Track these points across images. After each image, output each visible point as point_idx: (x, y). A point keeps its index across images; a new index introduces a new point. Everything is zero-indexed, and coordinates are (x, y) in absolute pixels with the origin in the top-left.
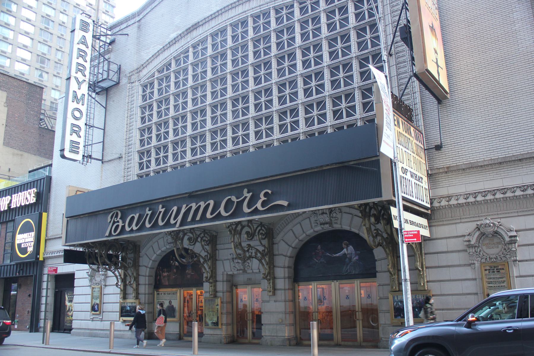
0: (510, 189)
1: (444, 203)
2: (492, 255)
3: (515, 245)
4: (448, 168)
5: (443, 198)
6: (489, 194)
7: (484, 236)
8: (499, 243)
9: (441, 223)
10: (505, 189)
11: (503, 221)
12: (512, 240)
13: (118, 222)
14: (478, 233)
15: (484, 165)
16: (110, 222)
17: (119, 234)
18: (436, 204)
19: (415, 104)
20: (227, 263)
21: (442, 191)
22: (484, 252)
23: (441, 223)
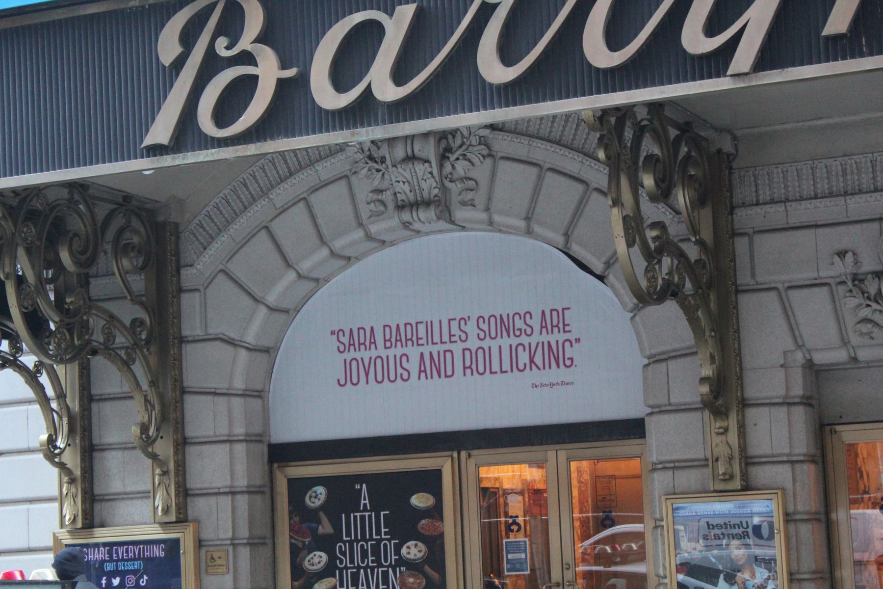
13: (247, 58)
16: (179, 63)
17: (261, 131)
20: (813, 309)
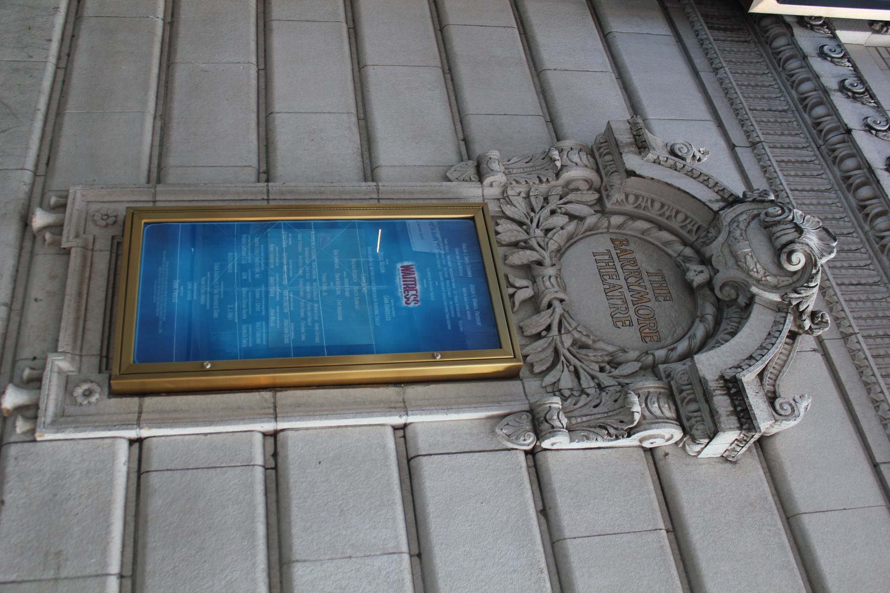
2: (558, 276)
8: (649, 330)
9: (700, 62)
12: (708, 397)
22: (572, 241)
23: (700, 62)
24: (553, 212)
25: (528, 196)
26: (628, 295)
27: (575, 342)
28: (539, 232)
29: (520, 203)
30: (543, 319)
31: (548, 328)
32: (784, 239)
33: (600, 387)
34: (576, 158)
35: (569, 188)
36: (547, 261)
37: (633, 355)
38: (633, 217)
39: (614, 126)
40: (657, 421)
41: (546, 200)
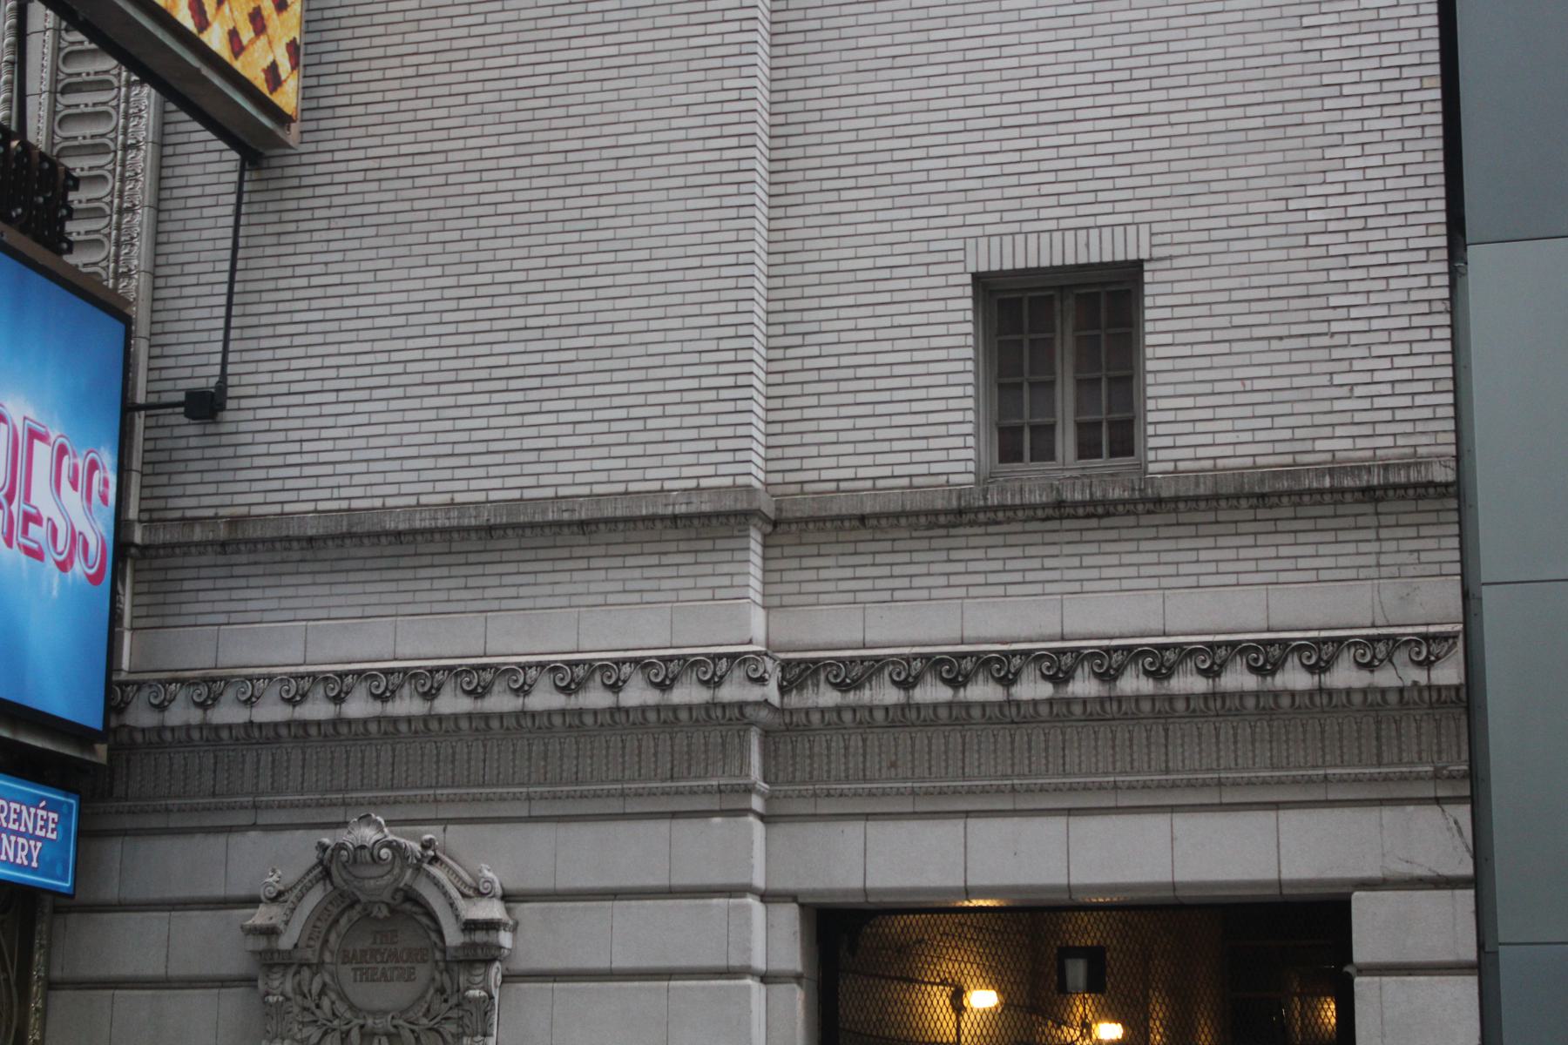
0: (410, 675)
1: (181, 714)
2: (374, 1013)
3: (486, 974)
4: (234, 521)
5: (183, 682)
6: (406, 690)
7: (355, 914)
9: (156, 822)
10: (484, 667)
11: (453, 838)
14: (315, 896)
15: (414, 532)
18: (141, 716)
19: (126, 148)
21: (194, 649)
22: (343, 997)
23: (156, 822)
24: (318, 1006)
25: (302, 1023)
26: (389, 965)
27: (425, 1015)
28: (336, 1022)
29: (307, 1031)
30: (406, 1034)
31: (413, 1031)
32: (368, 858)
33: (458, 1005)
34: (276, 983)
35: (299, 990)
36: (361, 1022)
37: (437, 976)
38: (326, 941)
39: (251, 948)
40: (486, 979)
41: (305, 1009)
